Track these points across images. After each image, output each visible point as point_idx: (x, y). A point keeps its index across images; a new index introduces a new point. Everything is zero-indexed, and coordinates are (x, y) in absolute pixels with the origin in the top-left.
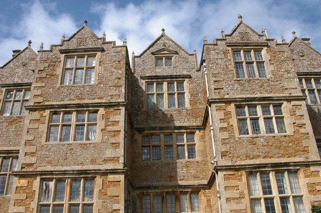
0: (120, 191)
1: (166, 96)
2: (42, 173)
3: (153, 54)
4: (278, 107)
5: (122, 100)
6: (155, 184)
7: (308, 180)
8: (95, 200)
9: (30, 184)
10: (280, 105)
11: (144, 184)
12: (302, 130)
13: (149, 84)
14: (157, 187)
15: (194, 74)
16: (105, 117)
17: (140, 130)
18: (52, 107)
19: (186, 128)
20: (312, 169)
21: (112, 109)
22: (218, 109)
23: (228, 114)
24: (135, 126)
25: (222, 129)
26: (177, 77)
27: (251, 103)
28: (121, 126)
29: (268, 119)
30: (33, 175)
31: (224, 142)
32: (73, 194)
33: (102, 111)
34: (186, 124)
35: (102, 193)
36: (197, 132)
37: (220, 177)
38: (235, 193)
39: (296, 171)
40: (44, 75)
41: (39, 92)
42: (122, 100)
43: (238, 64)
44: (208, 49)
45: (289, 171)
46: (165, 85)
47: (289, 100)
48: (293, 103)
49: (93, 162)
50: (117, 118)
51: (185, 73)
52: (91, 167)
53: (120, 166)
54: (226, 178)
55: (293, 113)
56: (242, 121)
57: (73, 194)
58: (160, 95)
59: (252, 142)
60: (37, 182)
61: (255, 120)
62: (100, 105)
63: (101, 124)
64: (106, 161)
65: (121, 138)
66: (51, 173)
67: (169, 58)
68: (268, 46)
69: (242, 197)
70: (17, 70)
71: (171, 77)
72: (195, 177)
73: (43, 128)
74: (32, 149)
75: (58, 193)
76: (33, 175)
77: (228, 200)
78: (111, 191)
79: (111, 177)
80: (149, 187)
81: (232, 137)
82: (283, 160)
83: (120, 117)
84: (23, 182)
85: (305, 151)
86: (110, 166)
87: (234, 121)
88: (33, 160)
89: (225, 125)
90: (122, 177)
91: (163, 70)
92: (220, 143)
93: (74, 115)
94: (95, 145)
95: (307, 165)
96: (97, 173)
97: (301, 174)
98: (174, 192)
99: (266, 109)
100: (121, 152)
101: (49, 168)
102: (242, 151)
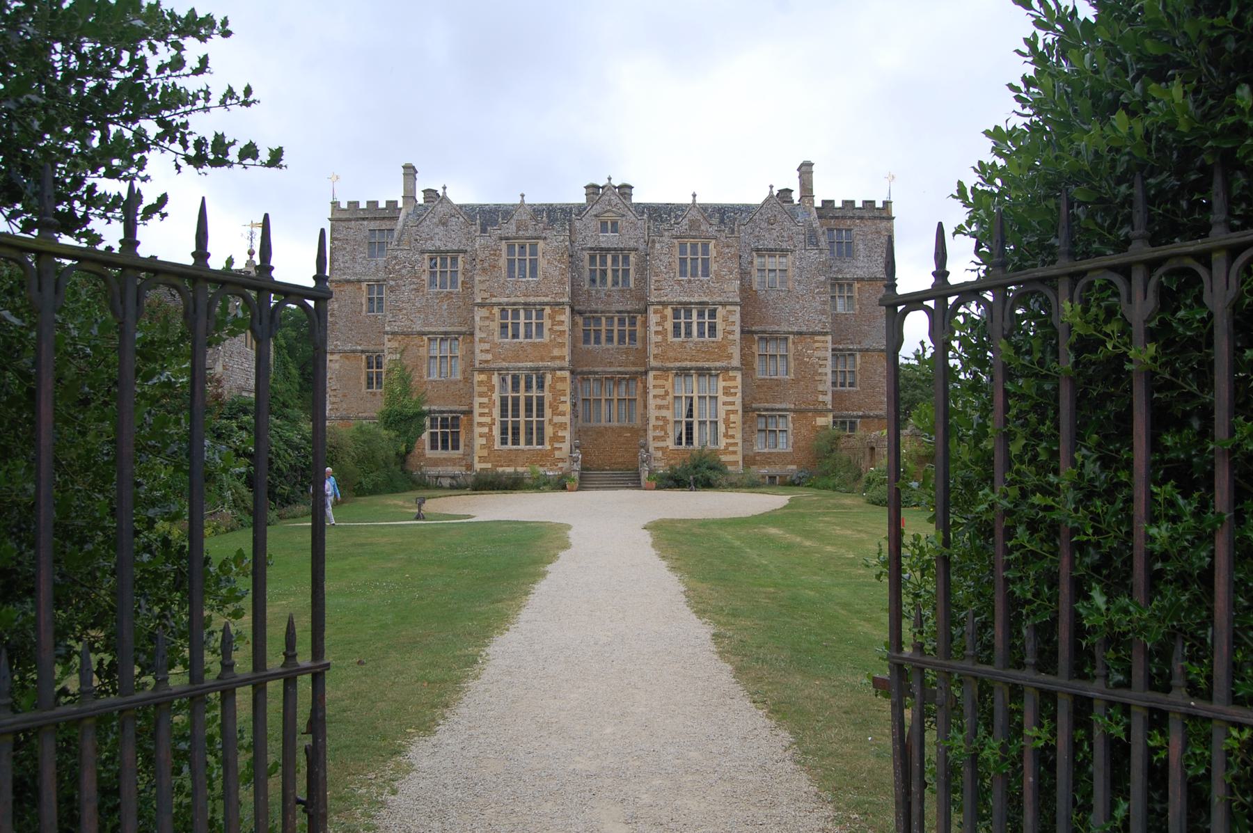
0: (567, 387)
1: (609, 273)
2: (499, 370)
3: (596, 216)
4: (713, 314)
5: (566, 299)
6: (596, 369)
7: (724, 384)
8: (547, 395)
9: (490, 379)
10: (715, 310)
11: (585, 369)
12: (731, 337)
13: (592, 258)
14: (597, 373)
15: (642, 247)
16: (552, 317)
17: (580, 313)
18: (500, 304)
19: (629, 312)
20: (731, 374)
21: (557, 308)
22: (655, 312)
23: (664, 318)
24: (576, 308)
25: (656, 333)
26: (622, 250)
27: (687, 307)
28: (566, 327)
29: (701, 325)
30: (491, 371)
31: (657, 344)
32: (528, 387)
33: (548, 310)
34: (629, 308)
35: (552, 387)
36: (639, 317)
37: (651, 374)
38: (661, 392)
39: (717, 375)
40: (486, 265)
41: (484, 287)
42: (566, 299)
43: (683, 261)
44: (654, 241)
45: (711, 375)
46: (609, 258)
47: (724, 304)
48: (729, 308)
49: (542, 359)
50: (562, 318)
51: (632, 244)
52: (541, 364)
53: (566, 364)
54: (655, 378)
55: (725, 320)
56: (676, 327)
57: (528, 387)
58: (604, 272)
59: (682, 344)
60: (496, 379)
61: (688, 325)
62: (547, 304)
63: (547, 323)
64: (554, 358)
65: (567, 339)
66: (507, 369)
67: (614, 224)
68: (716, 238)
69: (667, 393)
70: (437, 230)
71: (615, 249)
72: (634, 364)
73: (495, 326)
74: (487, 346)
75: (515, 387)
76: (491, 371)
77: (655, 397)
78: (560, 386)
79: (558, 373)
80: (590, 373)
81: (665, 340)
82: (706, 365)
83: (565, 317)
84: (483, 377)
85: (730, 357)
86: (558, 363)
87: (669, 325)
88: (489, 357)
89: (660, 328)
90: (567, 374)
91: (608, 239)
92: (653, 346)
93: (522, 313)
94: (544, 345)
95: (727, 369)
96: (547, 368)
97: (721, 377)
98: (612, 378)
99: (701, 315)
100: (566, 351)
101: (505, 364)
102: (671, 354)
